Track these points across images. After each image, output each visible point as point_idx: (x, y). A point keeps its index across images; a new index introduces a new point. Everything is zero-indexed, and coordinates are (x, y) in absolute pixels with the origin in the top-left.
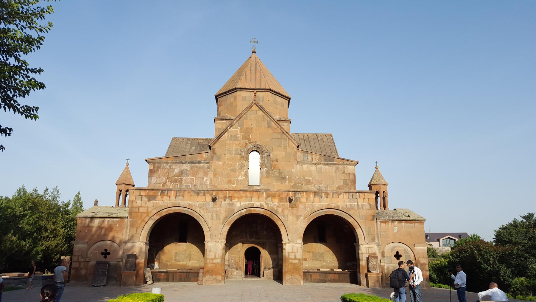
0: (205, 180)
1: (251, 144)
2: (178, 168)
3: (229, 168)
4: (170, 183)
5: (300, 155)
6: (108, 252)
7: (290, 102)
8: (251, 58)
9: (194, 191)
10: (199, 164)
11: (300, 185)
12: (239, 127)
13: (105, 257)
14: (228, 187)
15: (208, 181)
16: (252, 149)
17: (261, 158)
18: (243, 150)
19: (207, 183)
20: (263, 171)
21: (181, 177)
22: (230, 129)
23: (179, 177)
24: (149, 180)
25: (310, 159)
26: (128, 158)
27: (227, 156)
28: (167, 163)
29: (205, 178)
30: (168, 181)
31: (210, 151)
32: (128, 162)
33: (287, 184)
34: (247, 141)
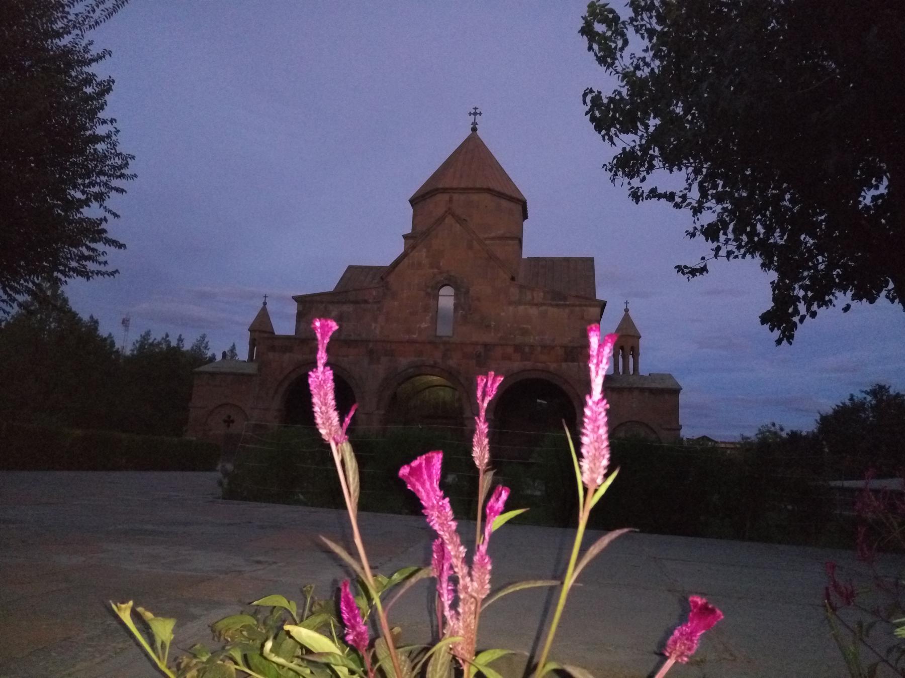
0: (373, 327)
3: (408, 311)
5: (514, 291)
11: (512, 336)
12: (425, 250)
13: (229, 426)
14: (407, 337)
25: (529, 297)
28: (322, 302)
29: (373, 325)
33: (493, 334)
34: (436, 270)
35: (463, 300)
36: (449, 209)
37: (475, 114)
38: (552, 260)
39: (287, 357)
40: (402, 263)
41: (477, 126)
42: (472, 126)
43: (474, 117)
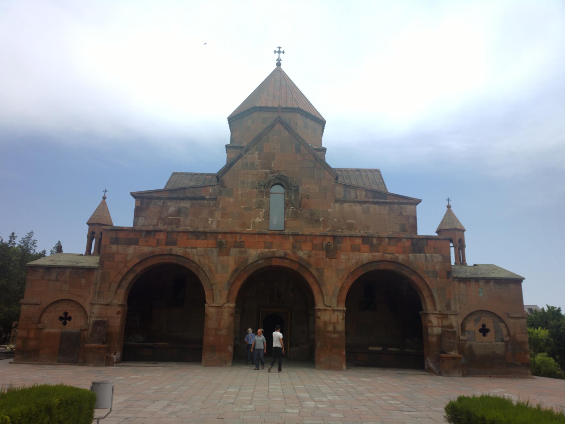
0: (210, 222)
1: (273, 175)
2: (174, 206)
4: (162, 225)
6: (68, 316)
7: (325, 128)
8: (275, 72)
9: (193, 233)
10: (203, 201)
11: (339, 230)
12: (257, 152)
13: (65, 324)
15: (214, 224)
16: (275, 182)
17: (287, 193)
18: (261, 183)
19: (213, 226)
20: (289, 211)
21: (178, 217)
22: (245, 155)
23: (176, 218)
24: (134, 221)
25: (353, 195)
26: (106, 189)
27: (240, 191)
28: (160, 198)
29: (210, 220)
30: (160, 222)
31: (217, 183)
32: (105, 195)
33: (322, 229)
34: (268, 171)
35: (293, 197)
36: (279, 117)
37: (279, 52)
38: (346, 170)
39: (131, 250)
40: (235, 164)
41: (281, 62)
42: (277, 62)
43: (278, 54)
